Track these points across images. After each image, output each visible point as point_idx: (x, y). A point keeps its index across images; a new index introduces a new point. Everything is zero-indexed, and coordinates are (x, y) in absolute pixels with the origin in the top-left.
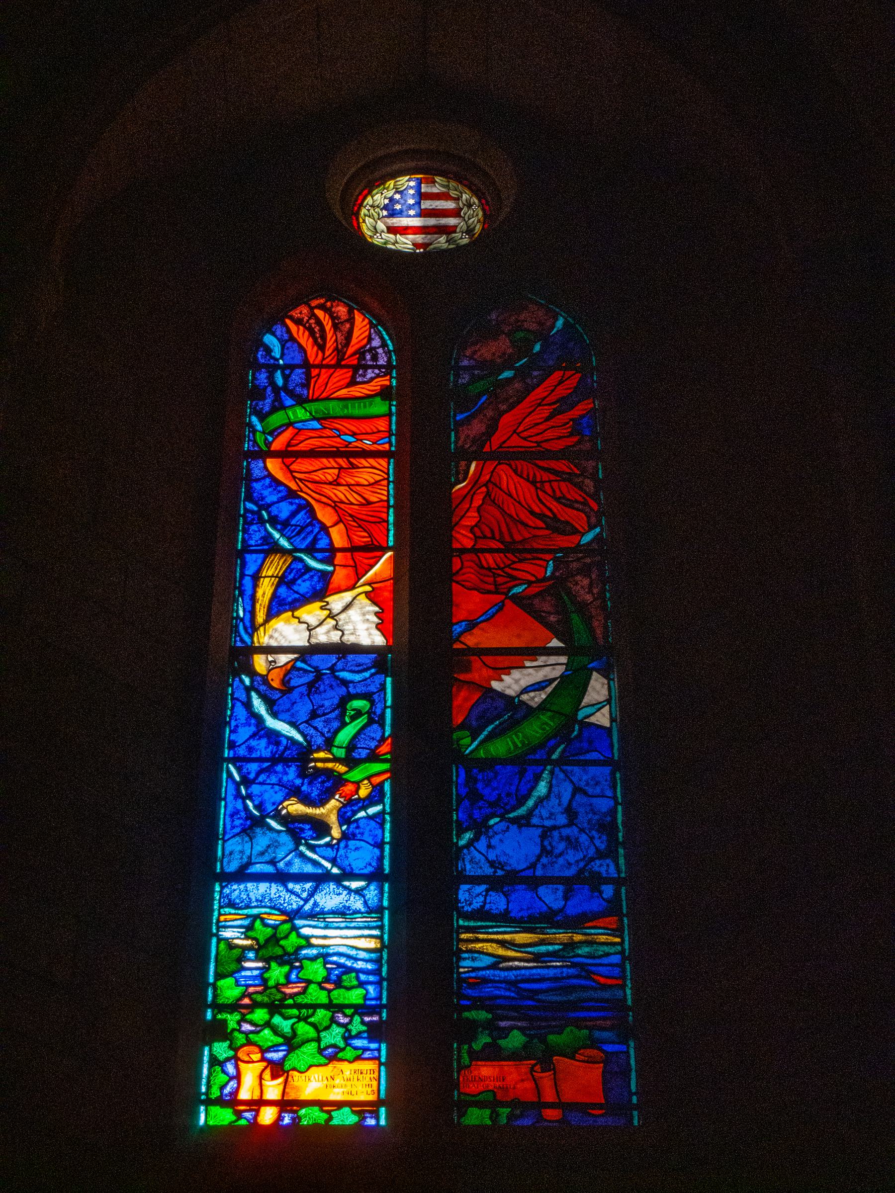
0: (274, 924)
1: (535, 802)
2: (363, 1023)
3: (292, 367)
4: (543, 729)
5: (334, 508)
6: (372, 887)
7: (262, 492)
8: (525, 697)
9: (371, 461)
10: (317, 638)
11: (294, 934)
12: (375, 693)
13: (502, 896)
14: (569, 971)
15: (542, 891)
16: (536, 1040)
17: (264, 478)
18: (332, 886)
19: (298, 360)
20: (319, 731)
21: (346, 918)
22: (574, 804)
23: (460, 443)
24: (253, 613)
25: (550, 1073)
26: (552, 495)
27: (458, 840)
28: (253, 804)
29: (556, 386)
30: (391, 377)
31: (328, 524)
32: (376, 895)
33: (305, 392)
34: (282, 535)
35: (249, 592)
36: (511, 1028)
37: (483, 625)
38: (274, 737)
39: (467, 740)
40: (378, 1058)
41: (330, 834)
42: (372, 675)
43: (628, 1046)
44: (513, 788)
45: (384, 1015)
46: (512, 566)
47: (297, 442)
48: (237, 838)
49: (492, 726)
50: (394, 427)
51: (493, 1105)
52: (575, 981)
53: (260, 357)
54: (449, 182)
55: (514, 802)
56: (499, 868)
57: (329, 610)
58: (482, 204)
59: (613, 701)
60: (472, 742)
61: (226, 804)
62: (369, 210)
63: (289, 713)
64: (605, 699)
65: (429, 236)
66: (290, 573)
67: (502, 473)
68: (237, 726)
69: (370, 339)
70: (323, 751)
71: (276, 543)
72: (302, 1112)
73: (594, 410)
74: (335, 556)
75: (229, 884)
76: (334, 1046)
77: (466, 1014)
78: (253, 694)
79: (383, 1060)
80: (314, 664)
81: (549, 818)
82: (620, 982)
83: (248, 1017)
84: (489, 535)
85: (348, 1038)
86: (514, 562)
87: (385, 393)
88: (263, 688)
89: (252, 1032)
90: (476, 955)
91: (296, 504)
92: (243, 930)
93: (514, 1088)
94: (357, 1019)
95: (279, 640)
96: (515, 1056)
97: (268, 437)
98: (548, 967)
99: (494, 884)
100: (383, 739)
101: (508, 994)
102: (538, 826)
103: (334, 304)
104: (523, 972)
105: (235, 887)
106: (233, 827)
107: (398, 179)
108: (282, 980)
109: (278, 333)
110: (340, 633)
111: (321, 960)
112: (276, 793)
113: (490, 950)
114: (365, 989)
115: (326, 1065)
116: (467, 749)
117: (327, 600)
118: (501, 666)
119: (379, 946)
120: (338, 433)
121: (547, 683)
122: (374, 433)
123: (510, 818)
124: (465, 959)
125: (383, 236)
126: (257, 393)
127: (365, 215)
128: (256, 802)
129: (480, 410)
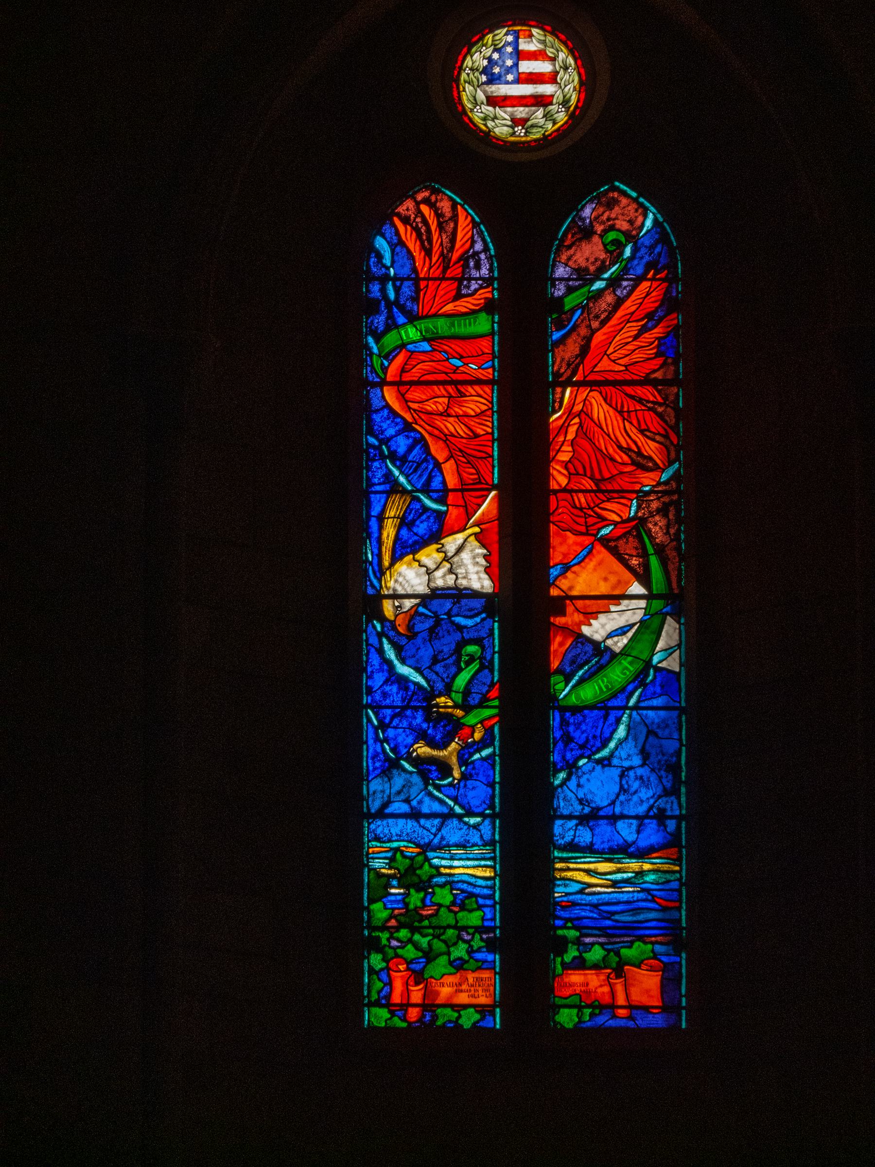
0: (411, 856)
1: (616, 744)
2: (482, 939)
3: (402, 280)
4: (625, 674)
5: (445, 441)
6: (487, 822)
7: (382, 424)
8: (609, 642)
9: (477, 388)
10: (435, 583)
11: (426, 865)
12: (484, 638)
13: (588, 830)
14: (639, 895)
15: (620, 824)
16: (612, 954)
17: (382, 408)
18: (455, 822)
19: (406, 271)
20: (440, 676)
21: (467, 851)
22: (647, 747)
23: (555, 368)
24: (380, 556)
25: (622, 980)
26: (637, 427)
27: (554, 780)
28: (389, 746)
29: (645, 298)
30: (493, 289)
31: (441, 461)
32: (490, 830)
33: (415, 307)
34: (402, 472)
35: (376, 535)
36: (593, 944)
37: (575, 569)
38: (403, 681)
39: (561, 685)
40: (494, 968)
41: (452, 775)
42: (483, 620)
43: (681, 957)
44: (599, 730)
45: (498, 932)
46: (616, 361)
47: (410, 367)
48: (379, 780)
49: (582, 671)
50: (496, 349)
51: (580, 1008)
52: (644, 904)
53: (372, 264)
54: (545, 35)
55: (598, 744)
56: (586, 806)
57: (445, 552)
58: (578, 67)
59: (683, 646)
60: (566, 685)
61: (368, 747)
62: (468, 74)
63: (414, 659)
64: (676, 643)
65: (527, 109)
66: (410, 514)
67: (593, 401)
68: (372, 672)
69: (473, 242)
70: (444, 696)
71: (396, 482)
72: (439, 1011)
73: (677, 327)
74: (448, 496)
75: (374, 820)
76: (460, 959)
77: (560, 932)
78: (385, 640)
79: (497, 970)
80: (433, 609)
81: (627, 759)
82: (677, 904)
83: (395, 935)
84: (581, 471)
85: (470, 952)
86: (604, 501)
87: (489, 307)
88: (392, 633)
89: (398, 947)
90: (567, 882)
91: (412, 437)
92: (387, 861)
93: (595, 991)
94: (477, 936)
95: (403, 584)
96: (596, 967)
97: (384, 361)
98: (623, 892)
99: (583, 820)
100: (492, 684)
101: (591, 915)
102: (617, 766)
103: (439, 198)
104: (603, 896)
105: (379, 823)
106: (375, 769)
107: (496, 32)
108: (419, 904)
109: (388, 235)
110: (454, 577)
111: (448, 887)
112: (407, 736)
113: (579, 878)
114: (483, 911)
115: (455, 974)
116: (561, 693)
117: (442, 541)
118: (589, 610)
119: (492, 874)
120: (446, 356)
121: (629, 628)
122: (479, 356)
123: (595, 759)
124: (559, 885)
125: (484, 111)
126: (372, 307)
127: (465, 82)
128: (392, 745)
129: (575, 328)
